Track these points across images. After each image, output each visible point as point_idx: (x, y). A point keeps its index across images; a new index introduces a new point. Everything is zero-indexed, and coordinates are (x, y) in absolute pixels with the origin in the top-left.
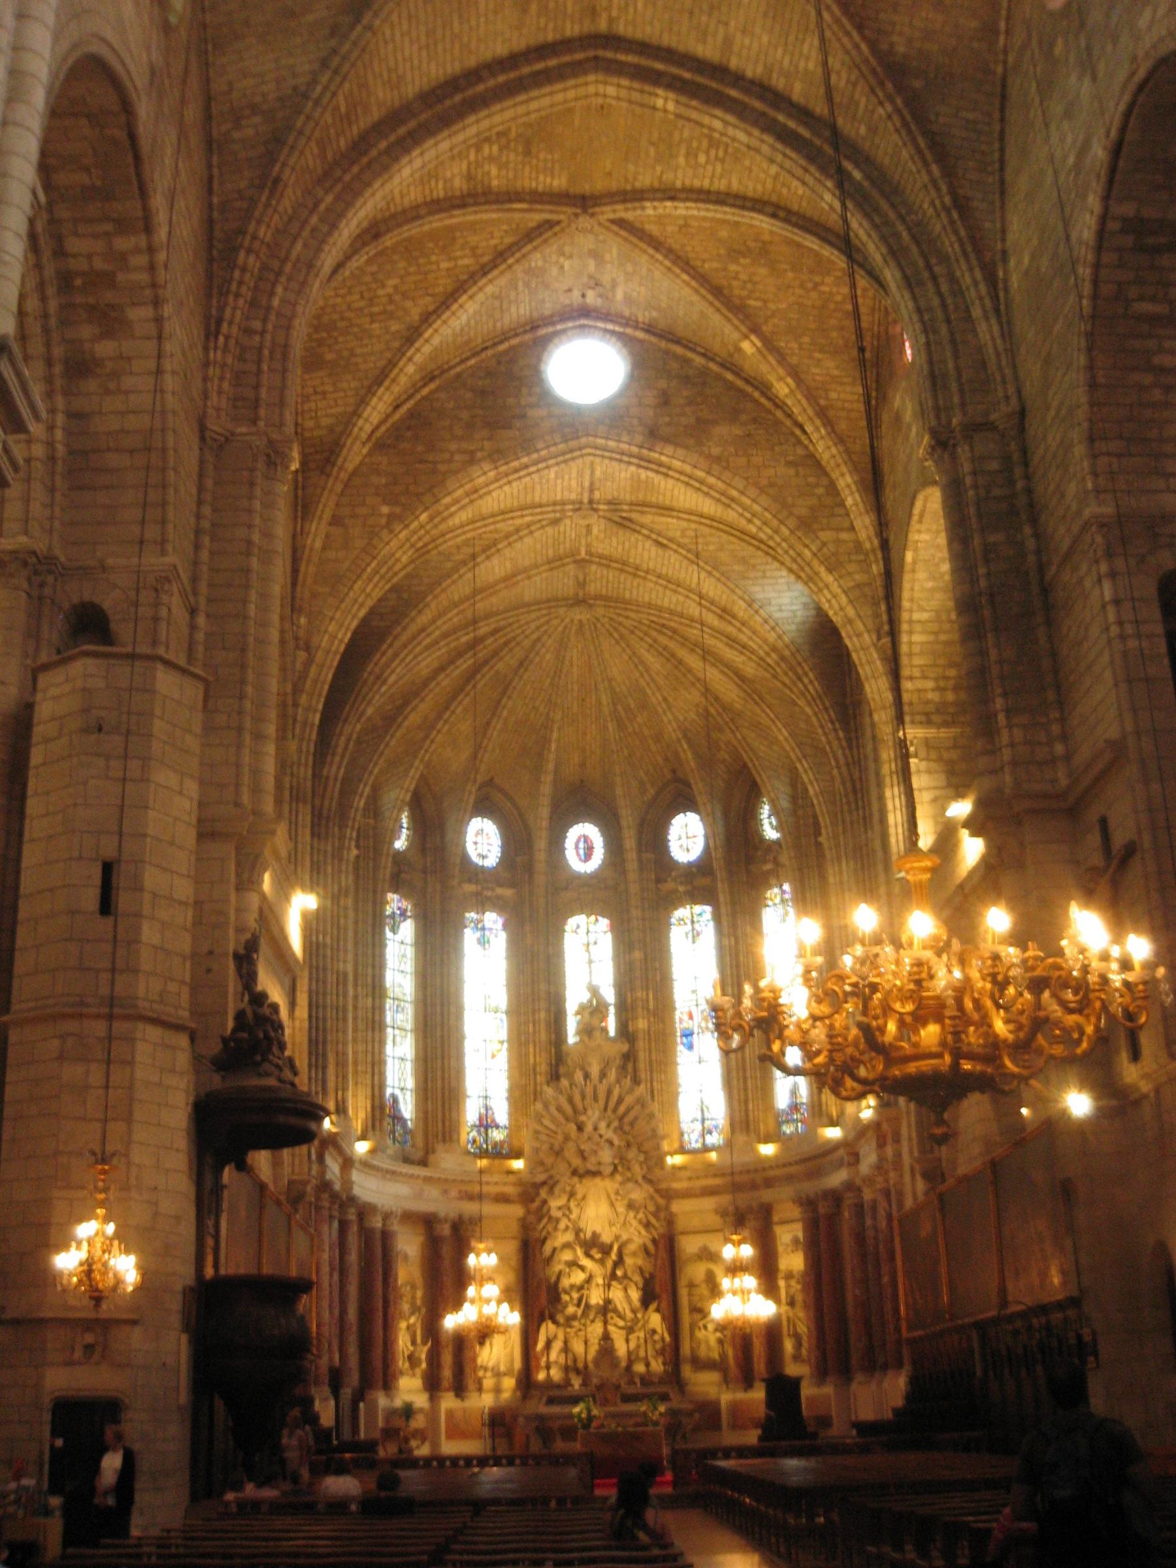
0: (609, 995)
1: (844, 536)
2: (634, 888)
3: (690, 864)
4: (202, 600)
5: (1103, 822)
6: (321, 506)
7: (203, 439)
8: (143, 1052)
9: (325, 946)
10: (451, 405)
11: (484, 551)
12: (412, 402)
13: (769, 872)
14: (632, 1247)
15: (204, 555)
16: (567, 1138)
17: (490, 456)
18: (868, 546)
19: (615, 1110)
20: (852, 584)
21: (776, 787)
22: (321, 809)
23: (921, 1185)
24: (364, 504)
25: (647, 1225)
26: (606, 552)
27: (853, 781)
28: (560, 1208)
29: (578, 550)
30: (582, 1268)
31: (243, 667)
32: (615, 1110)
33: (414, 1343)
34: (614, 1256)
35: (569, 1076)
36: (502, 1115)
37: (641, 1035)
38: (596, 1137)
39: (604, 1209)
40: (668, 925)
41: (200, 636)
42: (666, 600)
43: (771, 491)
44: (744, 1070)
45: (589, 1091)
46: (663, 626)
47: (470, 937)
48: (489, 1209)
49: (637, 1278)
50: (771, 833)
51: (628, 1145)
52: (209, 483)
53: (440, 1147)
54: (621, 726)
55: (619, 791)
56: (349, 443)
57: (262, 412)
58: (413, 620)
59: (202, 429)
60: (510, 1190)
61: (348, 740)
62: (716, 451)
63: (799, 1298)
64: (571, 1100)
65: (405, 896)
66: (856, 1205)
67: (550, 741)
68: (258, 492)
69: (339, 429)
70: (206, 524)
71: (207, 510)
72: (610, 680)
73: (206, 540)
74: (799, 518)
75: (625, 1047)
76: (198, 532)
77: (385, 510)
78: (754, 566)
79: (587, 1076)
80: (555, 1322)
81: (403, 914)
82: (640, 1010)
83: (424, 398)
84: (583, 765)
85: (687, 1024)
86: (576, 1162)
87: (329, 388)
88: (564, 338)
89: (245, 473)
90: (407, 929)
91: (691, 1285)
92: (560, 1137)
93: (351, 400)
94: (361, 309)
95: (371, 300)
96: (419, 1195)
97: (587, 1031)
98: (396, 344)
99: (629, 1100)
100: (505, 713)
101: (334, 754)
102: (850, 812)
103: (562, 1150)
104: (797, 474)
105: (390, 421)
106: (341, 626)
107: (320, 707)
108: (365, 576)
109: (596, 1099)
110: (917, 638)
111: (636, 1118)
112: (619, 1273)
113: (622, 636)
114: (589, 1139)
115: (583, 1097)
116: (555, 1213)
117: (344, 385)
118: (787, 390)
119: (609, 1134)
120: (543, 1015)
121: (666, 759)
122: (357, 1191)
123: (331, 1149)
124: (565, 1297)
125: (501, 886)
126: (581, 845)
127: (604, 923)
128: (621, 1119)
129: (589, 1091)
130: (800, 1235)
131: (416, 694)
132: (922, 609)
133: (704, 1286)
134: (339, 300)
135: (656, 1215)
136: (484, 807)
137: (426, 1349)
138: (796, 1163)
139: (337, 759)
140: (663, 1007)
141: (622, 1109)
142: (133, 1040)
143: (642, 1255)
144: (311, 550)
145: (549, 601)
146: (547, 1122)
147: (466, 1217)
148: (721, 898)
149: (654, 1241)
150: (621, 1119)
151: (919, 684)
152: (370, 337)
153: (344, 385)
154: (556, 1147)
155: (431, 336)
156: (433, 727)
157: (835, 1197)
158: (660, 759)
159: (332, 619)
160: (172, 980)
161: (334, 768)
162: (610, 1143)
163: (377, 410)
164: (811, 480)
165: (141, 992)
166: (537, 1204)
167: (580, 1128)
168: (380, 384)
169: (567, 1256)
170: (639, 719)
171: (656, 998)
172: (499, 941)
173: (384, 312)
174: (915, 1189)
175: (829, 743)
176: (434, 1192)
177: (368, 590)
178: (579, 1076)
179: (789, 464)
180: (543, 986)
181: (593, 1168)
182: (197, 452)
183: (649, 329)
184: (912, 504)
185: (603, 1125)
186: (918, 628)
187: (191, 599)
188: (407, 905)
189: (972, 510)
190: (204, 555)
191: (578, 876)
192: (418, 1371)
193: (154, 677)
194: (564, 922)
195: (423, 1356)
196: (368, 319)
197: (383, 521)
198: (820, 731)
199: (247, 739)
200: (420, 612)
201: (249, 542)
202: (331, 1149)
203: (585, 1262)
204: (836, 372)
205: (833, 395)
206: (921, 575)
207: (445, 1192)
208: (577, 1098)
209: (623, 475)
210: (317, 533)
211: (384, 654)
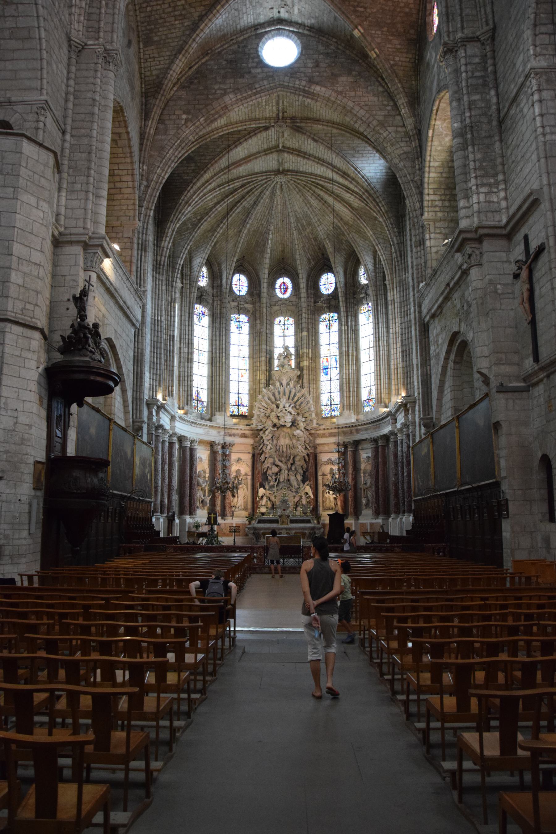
0: (292, 351)
1: (400, 129)
2: (304, 305)
3: (329, 295)
4: (69, 128)
5: (526, 238)
6: (153, 113)
7: (70, 46)
8: (9, 339)
9: (161, 321)
10: (216, 68)
11: (234, 143)
12: (197, 65)
13: (363, 298)
15: (70, 105)
16: (272, 411)
17: (233, 91)
18: (411, 133)
19: (292, 400)
20: (402, 152)
21: (367, 260)
22: (160, 261)
23: (423, 430)
24: (174, 114)
25: (306, 448)
26: (291, 147)
27: (400, 251)
29: (278, 146)
30: (277, 466)
31: (89, 161)
32: (292, 400)
33: (204, 495)
34: (291, 461)
35: (274, 385)
36: (245, 400)
37: (305, 368)
38: (284, 410)
40: (319, 322)
41: (67, 145)
42: (319, 170)
43: (366, 108)
44: (349, 383)
45: (281, 391)
46: (318, 184)
47: (233, 325)
48: (237, 440)
49: (301, 471)
50: (363, 281)
51: (298, 414)
52: (73, 69)
53: (217, 413)
54: (300, 233)
55: (298, 262)
56: (166, 82)
57: (101, 34)
58: (202, 176)
59: (69, 40)
60: (247, 432)
61: (173, 231)
62: (340, 89)
64: (274, 395)
65: (205, 306)
67: (268, 239)
68: (99, 75)
69: (161, 76)
70: (71, 90)
71: (72, 82)
72: (295, 211)
73: (71, 98)
74: (378, 121)
75: (299, 373)
76: (67, 93)
77: (184, 117)
78: (358, 151)
79: (281, 384)
80: (265, 488)
81: (203, 314)
82: (305, 358)
83: (203, 64)
84: (283, 251)
85: (326, 364)
86: (275, 421)
87: (156, 55)
88: (270, 35)
89: (93, 65)
90: (206, 321)
91: (324, 475)
92: (269, 410)
93: (167, 62)
94: (169, 13)
95: (174, 7)
96: (207, 434)
97: (282, 366)
98: (187, 33)
99: (298, 395)
100: (248, 226)
101: (166, 237)
102: (398, 265)
103: (269, 416)
104: (378, 101)
105: (187, 75)
106: (163, 170)
107: (153, 208)
108: (174, 147)
109: (284, 394)
110: (432, 175)
111: (302, 403)
112: (293, 468)
113: (300, 190)
115: (279, 394)
116: (266, 442)
117: (164, 54)
118: (375, 56)
119: (290, 409)
120: (263, 358)
121: (320, 249)
122: (177, 430)
123: (162, 410)
124: (269, 478)
125: (247, 303)
126: (282, 287)
127: (291, 320)
128: (295, 403)
129: (281, 391)
130: (370, 455)
131: (207, 214)
132: (435, 161)
134: (158, 7)
136: (239, 269)
137: (209, 498)
138: (370, 423)
139: (168, 239)
140: (315, 357)
141: (296, 399)
142: (4, 332)
144: (149, 133)
145: (266, 172)
146: (263, 404)
147: (228, 443)
148: (342, 309)
149: (308, 455)
150: (295, 403)
151: (432, 197)
152: (175, 28)
153: (164, 54)
154: (267, 415)
155: (204, 28)
156: (215, 231)
157: (386, 438)
158: (317, 249)
159: (159, 167)
160: (30, 303)
161: (166, 243)
163: (179, 65)
164: (385, 103)
165: (10, 308)
167: (278, 407)
168: (180, 53)
170: (308, 230)
171: (312, 353)
172: (246, 328)
173: (181, 15)
174: (420, 432)
175: (390, 234)
176: (214, 432)
177: (176, 154)
178: (278, 384)
179: (374, 95)
180: (264, 346)
181: (283, 424)
182: (67, 52)
183: (311, 28)
184: (433, 105)
185: (287, 405)
186: (433, 170)
187: (63, 126)
188: (205, 310)
189: (464, 84)
190: (70, 105)
191: (281, 300)
192: (206, 508)
193: (22, 146)
194: (274, 320)
196: (173, 19)
197: (183, 122)
198: (386, 229)
199: (91, 195)
200: (205, 172)
201: (94, 100)
202: (162, 410)
204: (399, 47)
205: (397, 59)
206: (435, 143)
207: (219, 432)
208: (277, 394)
209: (297, 104)
210: (152, 124)
211: (189, 191)
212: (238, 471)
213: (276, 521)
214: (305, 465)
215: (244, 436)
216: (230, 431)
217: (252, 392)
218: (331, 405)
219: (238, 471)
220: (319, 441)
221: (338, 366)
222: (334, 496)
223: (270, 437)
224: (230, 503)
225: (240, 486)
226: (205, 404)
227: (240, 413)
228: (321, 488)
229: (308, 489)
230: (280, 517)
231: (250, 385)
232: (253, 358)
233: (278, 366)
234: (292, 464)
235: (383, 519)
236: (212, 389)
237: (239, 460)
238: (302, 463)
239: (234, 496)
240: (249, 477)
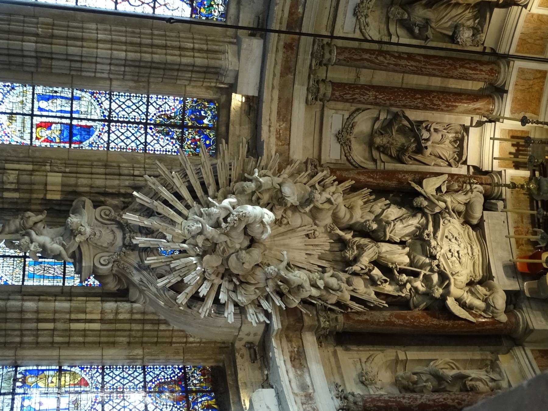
14: (343, 212)
32: (188, 207)
49: (378, 207)
85: (55, 132)
141: (185, 193)
149: (340, 181)
214: (366, 191)
217: (139, 352)
218: (183, 126)
221: (67, 93)
232: (21, 345)
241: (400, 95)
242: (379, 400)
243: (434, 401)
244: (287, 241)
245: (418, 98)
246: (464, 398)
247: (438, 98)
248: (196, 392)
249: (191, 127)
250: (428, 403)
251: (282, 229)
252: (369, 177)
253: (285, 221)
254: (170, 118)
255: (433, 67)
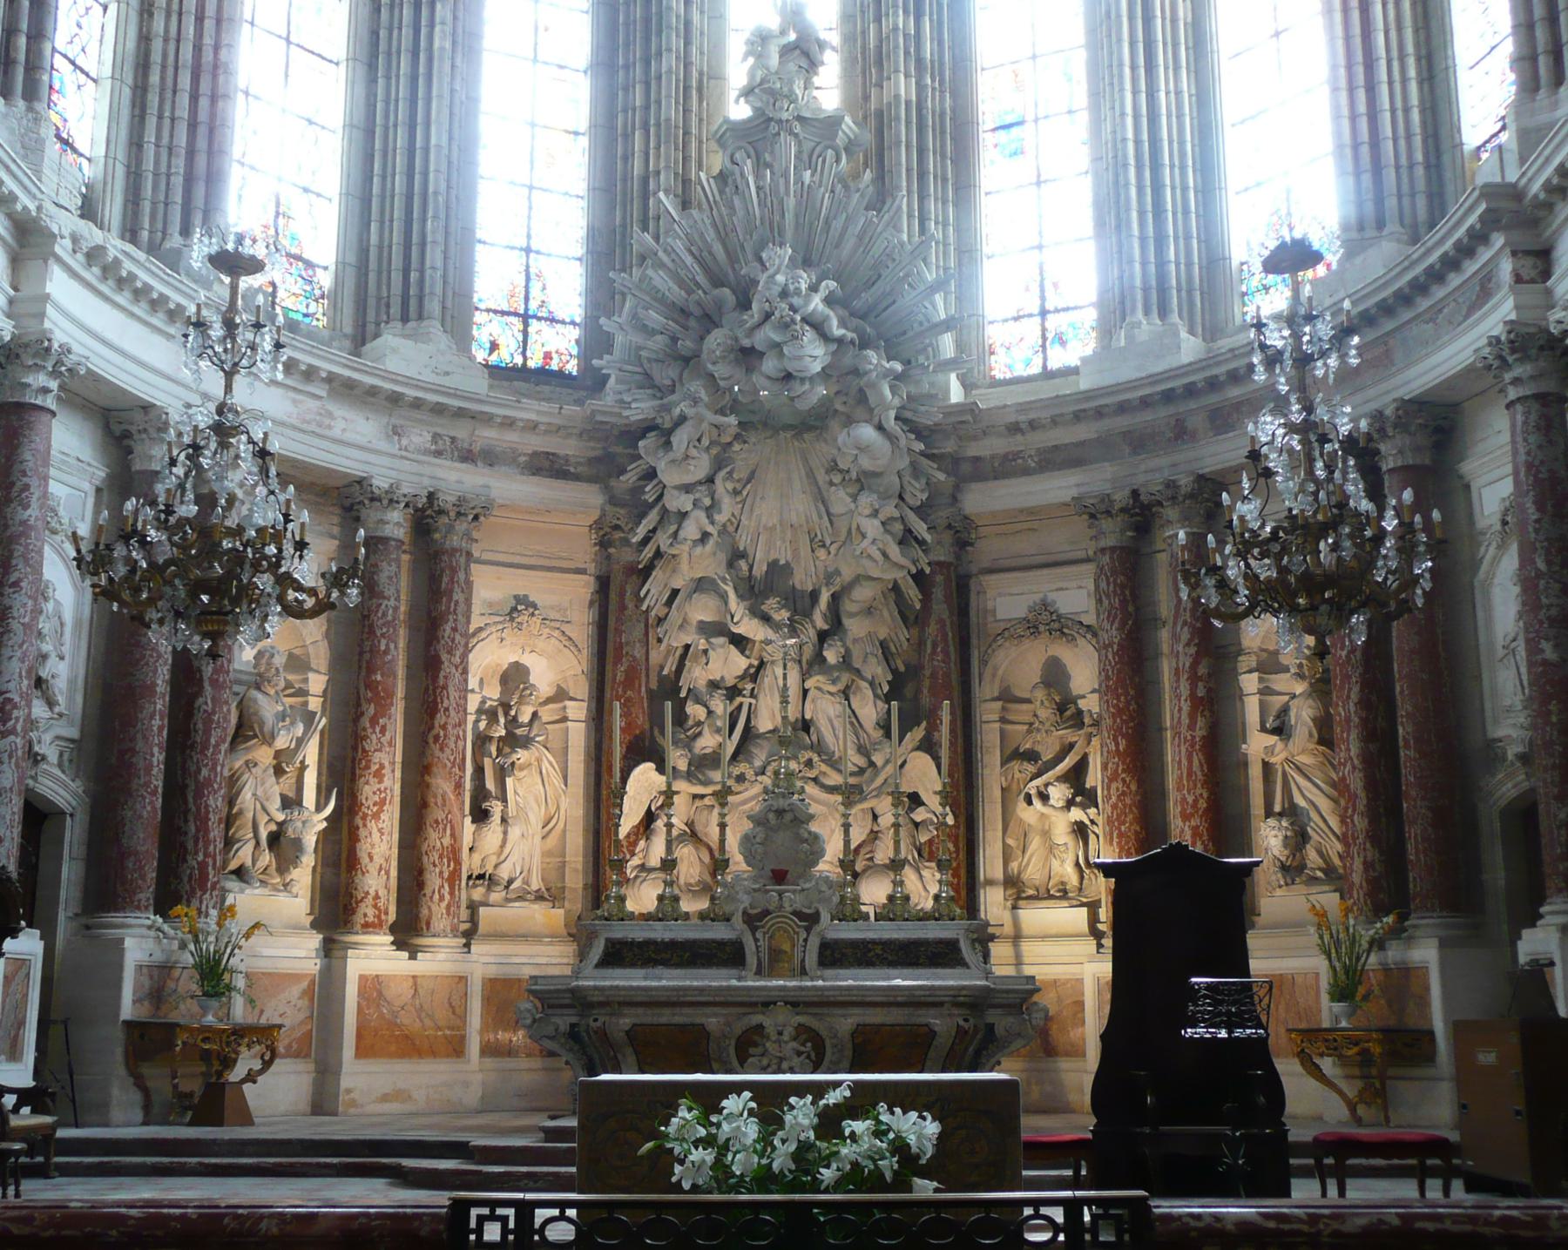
14: (863, 593)
25: (907, 538)
28: (687, 488)
30: (740, 642)
39: (801, 507)
49: (877, 669)
51: (864, 343)
60: (569, 448)
63: (1303, 715)
66: (1540, 398)
91: (1007, 697)
112: (831, 656)
114: (768, 316)
116: (677, 501)
122: (60, 331)
124: (695, 711)
133: (1040, 694)
135: (922, 511)
137: (319, 822)
143: (889, 613)
147: (447, 499)
149: (919, 578)
162: (818, 327)
166: (630, 478)
169: (702, 610)
195: (310, 840)
203: (748, 627)
212: (514, 677)
213: (729, 955)
215: (548, 467)
216: (461, 431)
218: (1044, 313)
219: (514, 677)
220: (981, 500)
222: (1076, 814)
223: (700, 468)
224: (454, 854)
225: (522, 755)
226: (326, 280)
227: (534, 362)
228: (992, 776)
229: (925, 776)
230: (753, 921)
231: (591, 208)
233: (747, 93)
234: (823, 637)
235: (1443, 944)
236: (366, 201)
237: (519, 608)
238: (886, 625)
239: (480, 816)
240: (578, 711)
241: (1118, 699)
242: (452, 581)
243: (445, 687)
244: (797, 485)
245: (1117, 744)
246: (448, 751)
247: (1124, 794)
248: (525, 333)
249: (1044, 330)
250: (442, 674)
251: (821, 477)
252: (935, 645)
253: (837, 479)
254: (1056, 285)
255: (1185, 762)
